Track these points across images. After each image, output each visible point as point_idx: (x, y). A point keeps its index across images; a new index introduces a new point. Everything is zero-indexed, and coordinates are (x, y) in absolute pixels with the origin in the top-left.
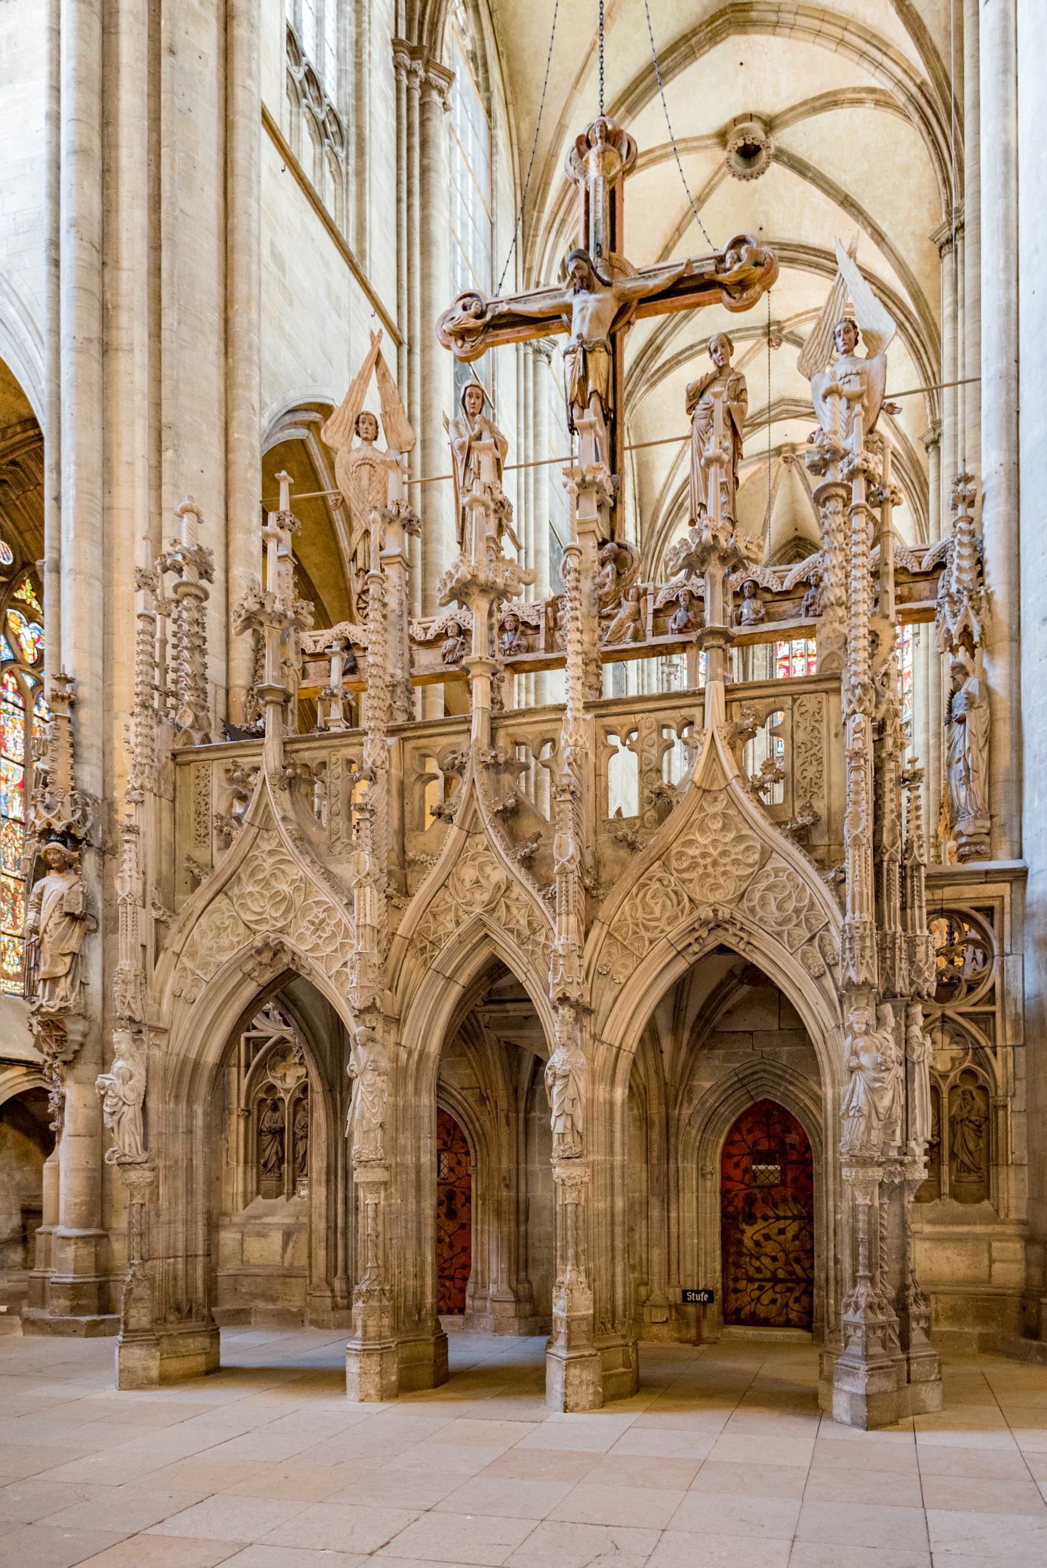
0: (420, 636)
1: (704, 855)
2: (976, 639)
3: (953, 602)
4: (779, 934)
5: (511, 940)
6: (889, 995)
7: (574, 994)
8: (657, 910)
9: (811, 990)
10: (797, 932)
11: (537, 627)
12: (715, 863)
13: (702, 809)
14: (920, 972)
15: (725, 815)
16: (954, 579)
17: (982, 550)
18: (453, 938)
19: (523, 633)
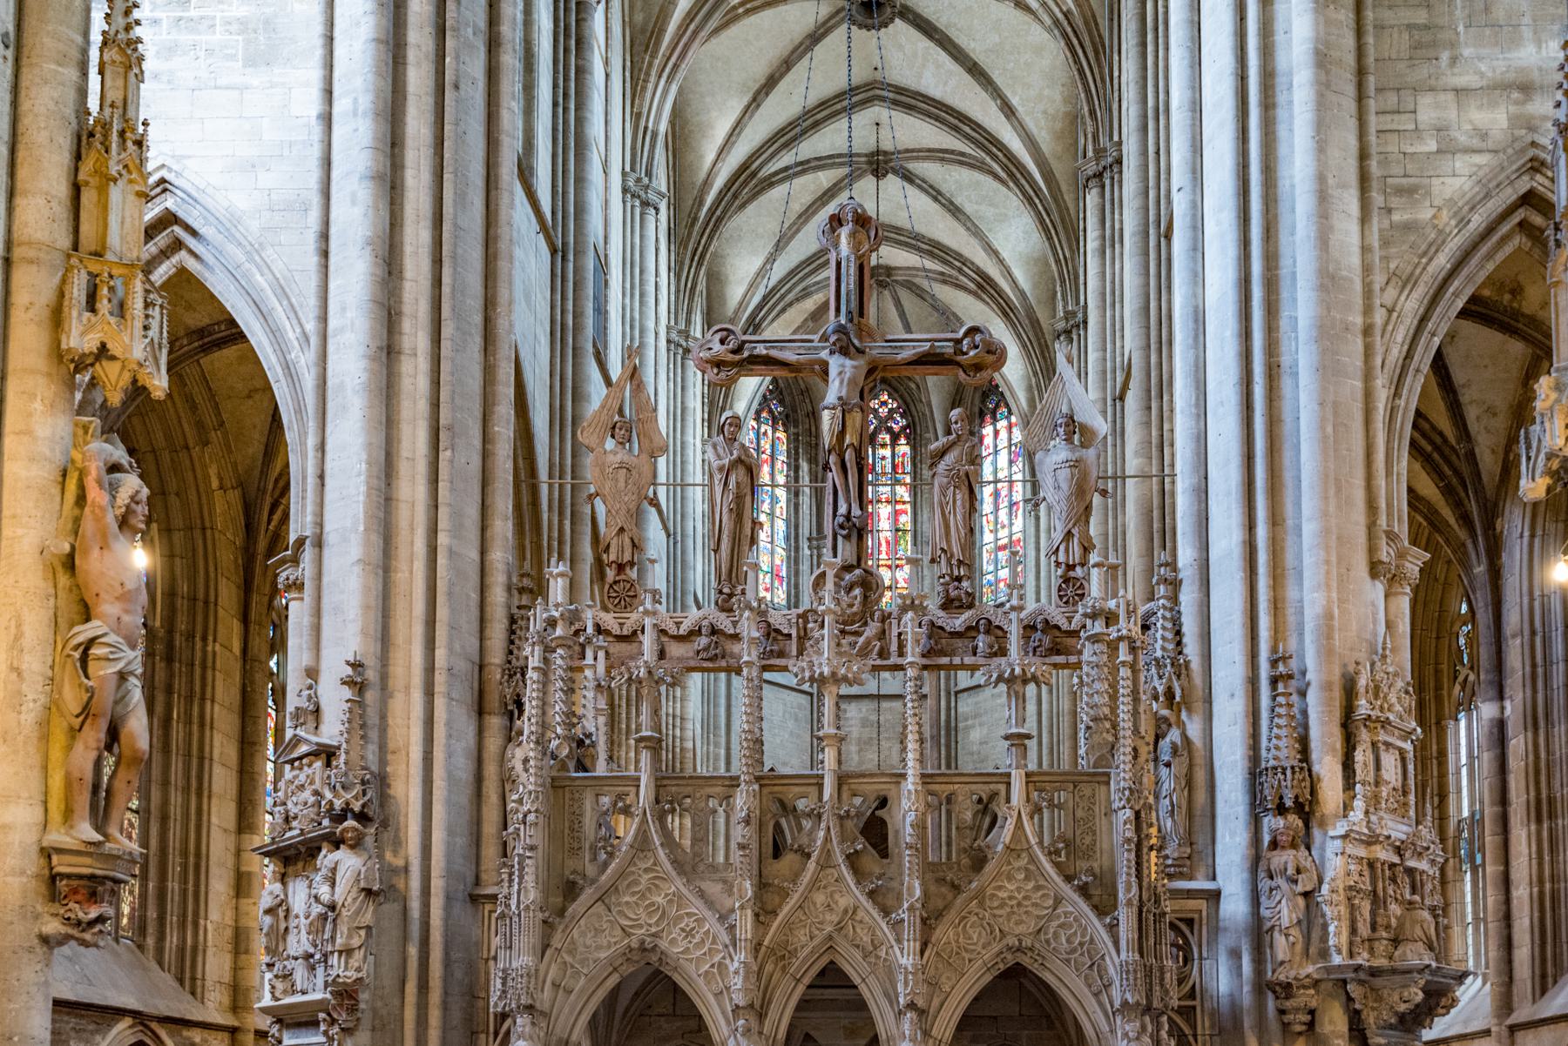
0: (673, 631)
1: (1011, 898)
2: (1178, 699)
3: (1158, 666)
4: (1068, 961)
5: (858, 955)
6: (1148, 1009)
7: (920, 1003)
8: (975, 937)
9: (1091, 1003)
10: (1081, 959)
11: (789, 635)
12: (1019, 904)
13: (1009, 863)
14: (1167, 992)
15: (1027, 869)
16: (1159, 641)
17: (1181, 625)
18: (806, 951)
19: (775, 639)
